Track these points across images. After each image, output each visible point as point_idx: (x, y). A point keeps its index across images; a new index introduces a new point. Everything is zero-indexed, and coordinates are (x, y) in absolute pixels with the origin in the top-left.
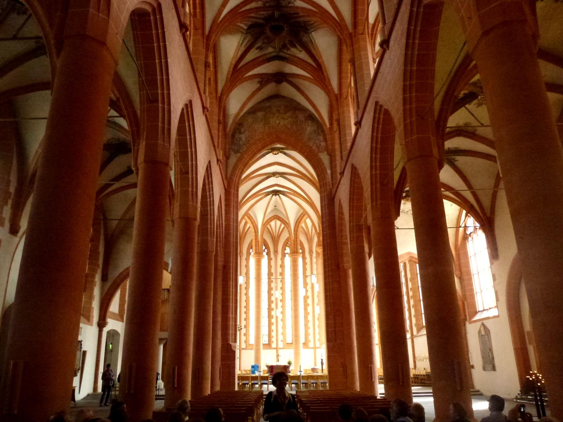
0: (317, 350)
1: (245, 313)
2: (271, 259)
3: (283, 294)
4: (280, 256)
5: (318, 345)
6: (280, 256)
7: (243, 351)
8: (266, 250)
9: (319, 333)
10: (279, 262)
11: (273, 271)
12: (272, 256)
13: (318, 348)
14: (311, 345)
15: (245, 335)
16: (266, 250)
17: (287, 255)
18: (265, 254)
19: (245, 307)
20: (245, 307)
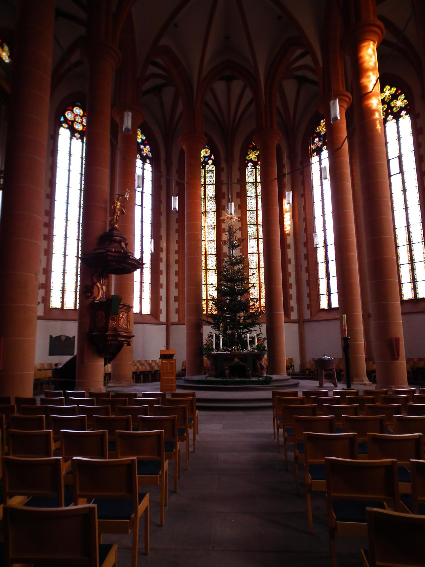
0: (306, 324)
1: (177, 262)
2: (222, 170)
3: (243, 219)
4: (236, 165)
5: (307, 315)
6: (236, 165)
7: (173, 328)
8: (212, 157)
9: (309, 295)
10: (236, 175)
11: (224, 189)
12: (223, 165)
13: (308, 321)
14: (294, 315)
15: (176, 299)
16: (212, 157)
17: (250, 164)
18: (210, 162)
19: (176, 252)
20: (176, 252)
